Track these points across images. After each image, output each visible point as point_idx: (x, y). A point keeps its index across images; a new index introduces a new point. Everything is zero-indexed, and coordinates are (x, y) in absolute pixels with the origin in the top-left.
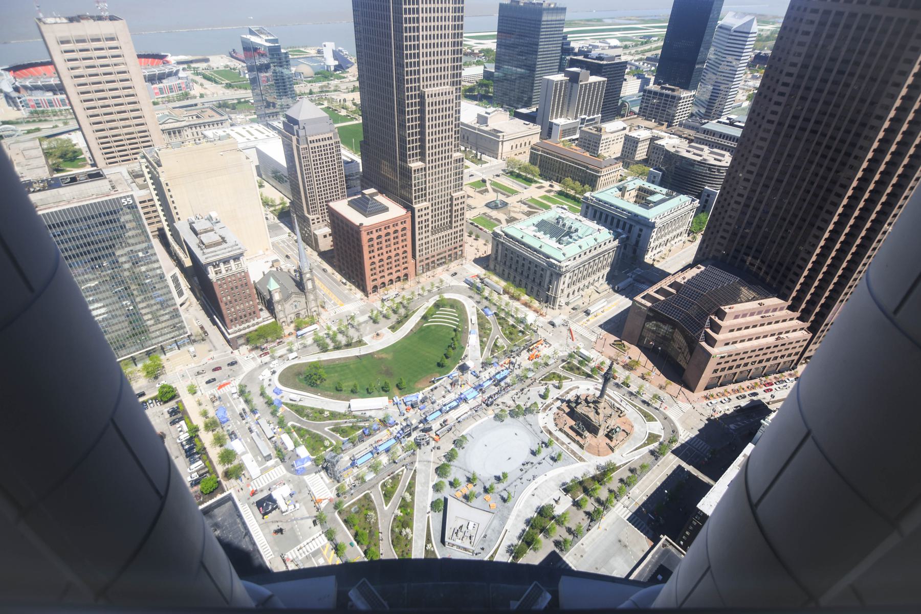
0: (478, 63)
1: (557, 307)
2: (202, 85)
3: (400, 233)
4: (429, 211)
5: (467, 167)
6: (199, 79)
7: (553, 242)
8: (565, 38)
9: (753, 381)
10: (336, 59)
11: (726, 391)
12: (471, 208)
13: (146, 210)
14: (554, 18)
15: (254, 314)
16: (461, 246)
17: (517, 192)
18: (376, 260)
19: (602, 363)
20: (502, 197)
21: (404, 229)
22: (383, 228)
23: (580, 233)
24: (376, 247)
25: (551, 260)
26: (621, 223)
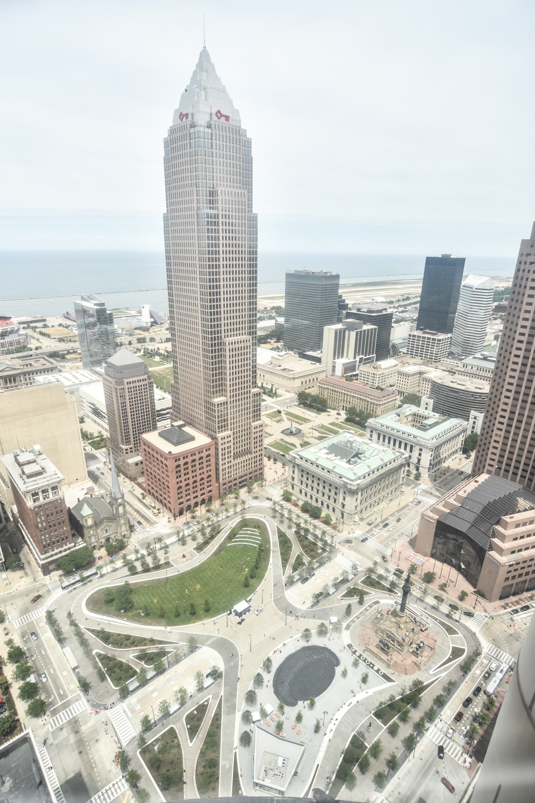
0: (271, 318)
2: (38, 340)
3: (204, 460)
4: (232, 439)
6: (37, 336)
8: (341, 297)
10: (152, 317)
11: (520, 599)
14: (331, 283)
16: (261, 469)
17: (308, 420)
18: (183, 484)
20: (295, 425)
21: (208, 456)
22: (189, 455)
23: (367, 454)
24: (183, 472)
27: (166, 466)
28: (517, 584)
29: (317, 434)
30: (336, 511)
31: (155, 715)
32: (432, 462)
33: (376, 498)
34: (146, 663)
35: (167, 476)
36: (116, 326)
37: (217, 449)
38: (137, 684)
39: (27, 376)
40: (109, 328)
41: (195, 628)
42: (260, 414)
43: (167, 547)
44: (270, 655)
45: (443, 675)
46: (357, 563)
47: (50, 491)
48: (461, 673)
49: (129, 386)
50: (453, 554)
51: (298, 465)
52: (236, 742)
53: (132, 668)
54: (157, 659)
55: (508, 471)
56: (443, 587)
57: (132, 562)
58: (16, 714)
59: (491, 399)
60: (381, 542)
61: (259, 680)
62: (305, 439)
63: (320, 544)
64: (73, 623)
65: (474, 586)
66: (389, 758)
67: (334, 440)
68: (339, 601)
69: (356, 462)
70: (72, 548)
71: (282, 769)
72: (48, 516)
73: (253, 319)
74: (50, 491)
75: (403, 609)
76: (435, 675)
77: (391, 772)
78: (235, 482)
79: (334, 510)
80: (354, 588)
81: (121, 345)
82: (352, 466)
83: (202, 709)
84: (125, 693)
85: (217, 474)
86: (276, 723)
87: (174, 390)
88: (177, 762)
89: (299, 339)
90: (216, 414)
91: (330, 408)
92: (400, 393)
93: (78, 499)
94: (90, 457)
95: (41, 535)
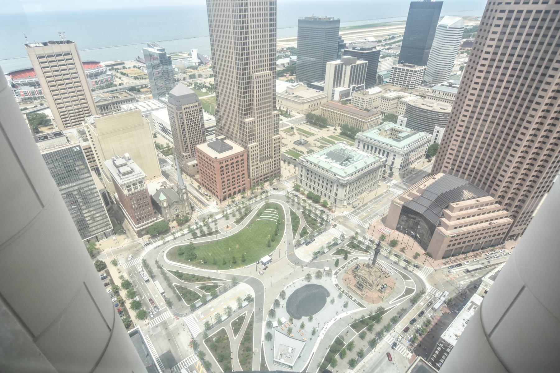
2: (120, 78)
3: (240, 163)
5: (281, 120)
6: (119, 75)
9: (475, 253)
10: (199, 58)
11: (457, 259)
13: (88, 154)
16: (279, 169)
17: (313, 134)
20: (303, 138)
21: (242, 160)
23: (355, 159)
25: (337, 176)
28: (456, 249)
29: (319, 144)
31: (213, 321)
32: (402, 165)
33: (360, 190)
34: (206, 291)
36: (174, 66)
37: (248, 155)
38: (201, 303)
39: (115, 105)
40: (169, 68)
41: (236, 272)
43: (216, 221)
44: (284, 289)
45: (398, 304)
46: (344, 233)
47: (138, 184)
48: (411, 304)
49: (186, 111)
50: (412, 229)
52: (263, 338)
53: (197, 294)
54: (213, 290)
55: (459, 171)
56: (403, 250)
57: (194, 230)
58: (129, 317)
59: (451, 118)
60: (362, 220)
61: (277, 303)
62: (311, 148)
63: (319, 220)
64: (160, 267)
65: (425, 249)
66: (359, 351)
67: (332, 148)
68: (331, 257)
69: (346, 164)
71: (291, 354)
72: (138, 200)
73: (273, 58)
74: (138, 184)
75: (374, 262)
76: (393, 304)
77: (360, 359)
79: (329, 197)
80: (341, 249)
81: (178, 80)
83: (242, 319)
84: (194, 308)
85: (249, 173)
86: (287, 329)
87: (217, 114)
88: (227, 347)
89: (307, 73)
90: (247, 131)
91: (330, 125)
92: (382, 113)
94: (162, 162)
95: (135, 213)
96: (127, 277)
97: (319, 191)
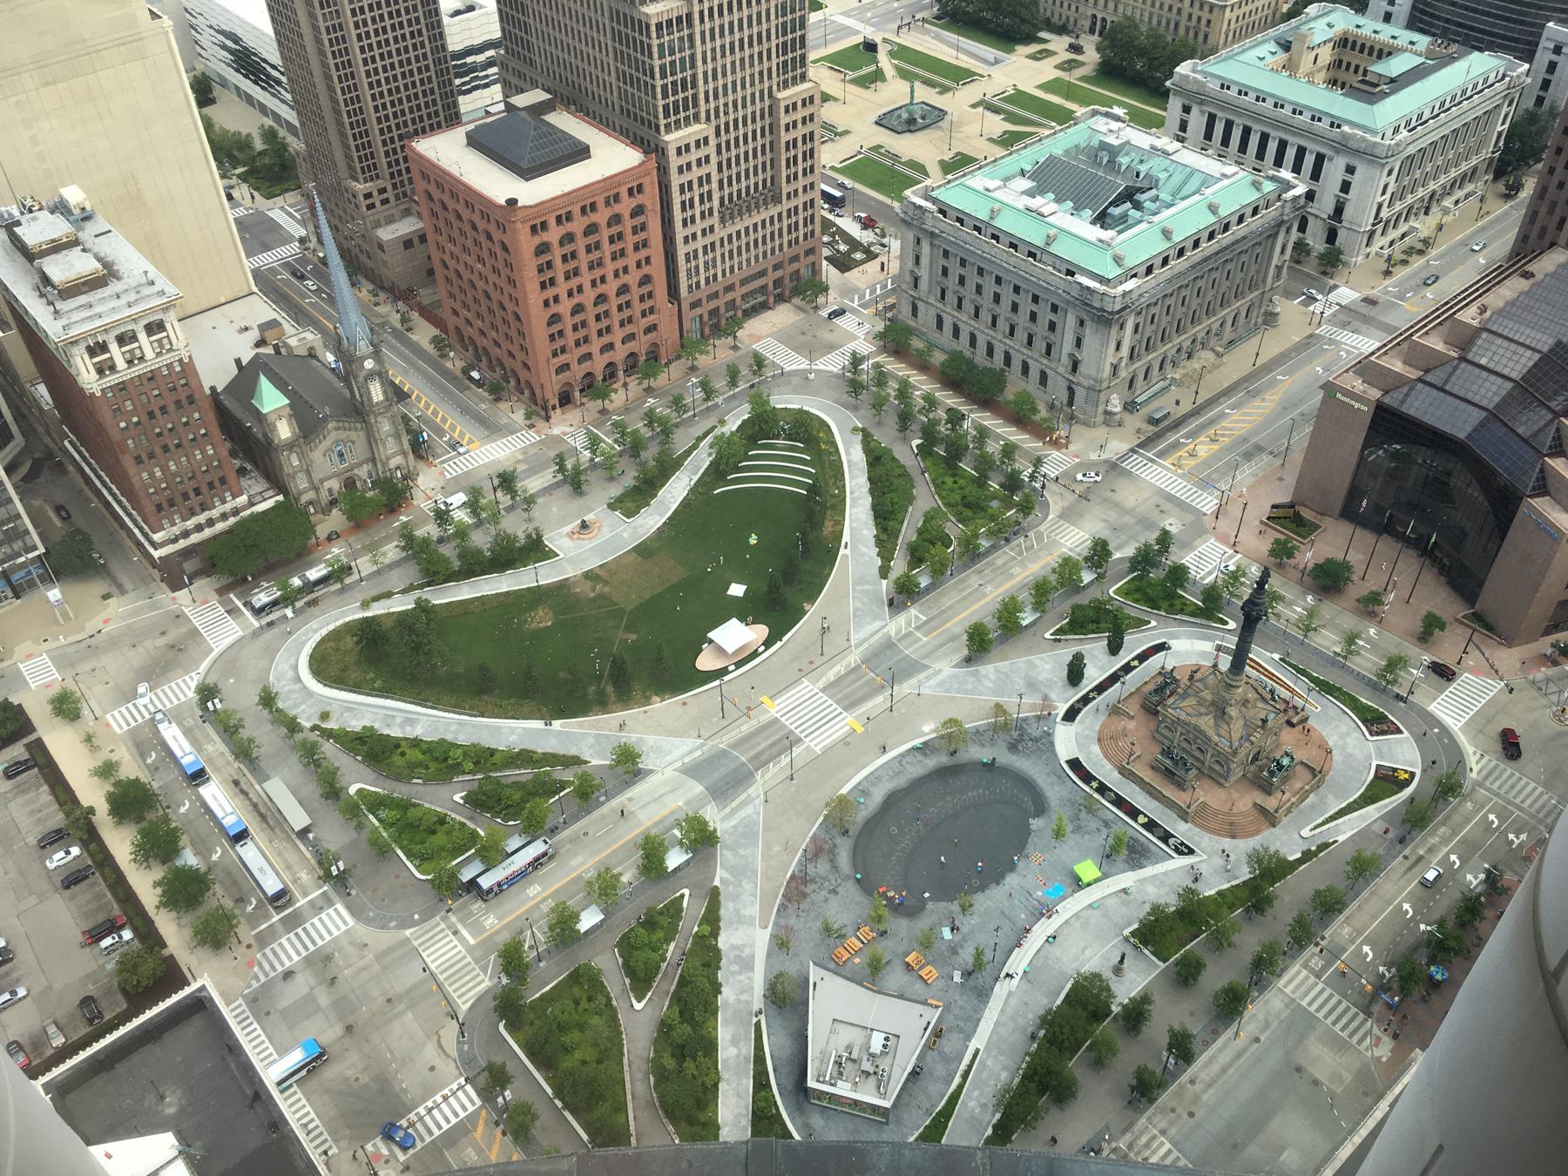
1: (1100, 418)
4: (711, 150)
7: (1082, 226)
12: (833, 132)
15: (219, 485)
18: (565, 307)
19: (1235, 577)
20: (924, 94)
21: (638, 211)
26: (1291, 154)
27: (505, 248)
29: (997, 125)
30: (1049, 382)
33: (1184, 340)
35: (512, 282)
37: (664, 189)
42: (803, 57)
43: (530, 501)
47: (142, 336)
51: (932, 235)
67: (1057, 143)
69: (1124, 218)
70: (244, 508)
78: (729, 296)
82: (1111, 233)
83: (660, 921)
93: (238, 362)
96: (130, 769)
97: (992, 352)
